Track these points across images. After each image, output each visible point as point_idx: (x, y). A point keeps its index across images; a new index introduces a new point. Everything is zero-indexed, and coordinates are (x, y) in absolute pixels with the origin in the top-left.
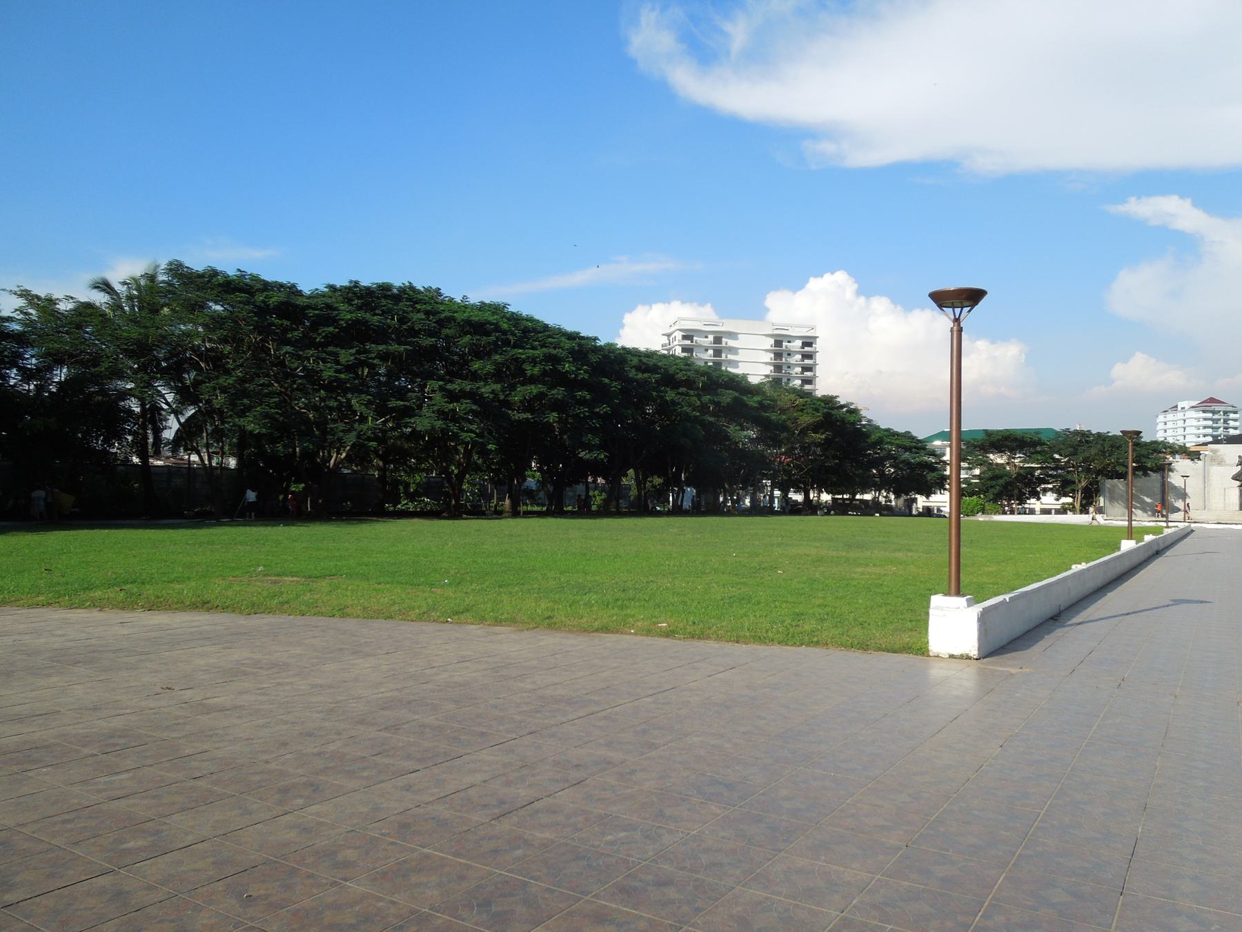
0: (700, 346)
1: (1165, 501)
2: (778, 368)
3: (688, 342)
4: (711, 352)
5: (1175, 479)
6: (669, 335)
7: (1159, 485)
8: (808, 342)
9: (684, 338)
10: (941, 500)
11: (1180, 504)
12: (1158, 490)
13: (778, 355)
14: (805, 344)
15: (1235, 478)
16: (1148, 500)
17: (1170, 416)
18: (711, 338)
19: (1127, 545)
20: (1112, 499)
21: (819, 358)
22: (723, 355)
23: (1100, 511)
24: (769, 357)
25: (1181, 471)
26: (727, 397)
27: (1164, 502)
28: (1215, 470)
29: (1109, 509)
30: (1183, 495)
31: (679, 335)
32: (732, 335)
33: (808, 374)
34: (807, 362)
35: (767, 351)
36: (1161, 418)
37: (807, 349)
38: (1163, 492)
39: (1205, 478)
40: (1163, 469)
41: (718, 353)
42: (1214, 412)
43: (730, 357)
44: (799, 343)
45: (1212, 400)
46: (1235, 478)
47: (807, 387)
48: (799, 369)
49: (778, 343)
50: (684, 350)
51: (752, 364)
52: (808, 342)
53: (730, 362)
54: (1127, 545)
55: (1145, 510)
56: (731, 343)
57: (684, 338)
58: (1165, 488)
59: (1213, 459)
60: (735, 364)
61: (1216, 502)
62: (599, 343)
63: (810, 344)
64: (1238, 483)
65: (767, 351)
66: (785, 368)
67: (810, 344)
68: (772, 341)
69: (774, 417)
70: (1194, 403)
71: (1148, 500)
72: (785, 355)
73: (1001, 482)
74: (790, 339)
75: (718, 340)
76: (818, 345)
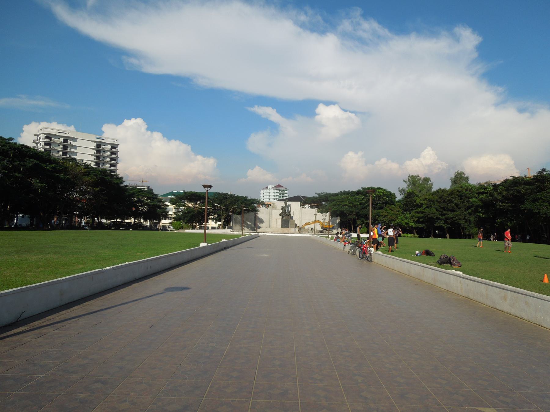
0: (55, 143)
1: (256, 224)
2: (98, 158)
3: (49, 140)
5: (260, 215)
6: (37, 136)
7: (253, 217)
8: (114, 147)
10: (165, 223)
11: (260, 225)
12: (253, 220)
13: (98, 151)
14: (112, 148)
15: (280, 215)
16: (249, 223)
17: (265, 191)
18: (62, 139)
19: (203, 244)
20: (236, 223)
21: (119, 155)
22: (69, 149)
23: (230, 228)
24: (93, 152)
25: (262, 212)
26: (30, 163)
27: (255, 224)
28: (274, 211)
29: (234, 227)
30: (262, 222)
31: (43, 136)
33: (114, 162)
34: (113, 156)
35: (92, 149)
36: (262, 192)
37: (113, 150)
38: (255, 220)
39: (270, 215)
40: (255, 211)
41: (65, 147)
42: (280, 190)
43: (72, 150)
44: (109, 147)
45: (279, 186)
46: (280, 215)
47: (112, 168)
48: (109, 159)
49: (99, 145)
50: (46, 144)
51: (85, 154)
52: (114, 147)
53: (72, 152)
54: (203, 244)
55: (248, 228)
56: (73, 143)
57: (46, 138)
59: (273, 207)
60: (75, 154)
61: (273, 224)
63: (115, 148)
64: (281, 217)
65: (92, 149)
66: (102, 158)
67: (115, 148)
68: (95, 144)
69: (62, 176)
70: (273, 186)
71: (249, 223)
73: (190, 214)
74: (105, 144)
75: (66, 141)
76: (119, 149)
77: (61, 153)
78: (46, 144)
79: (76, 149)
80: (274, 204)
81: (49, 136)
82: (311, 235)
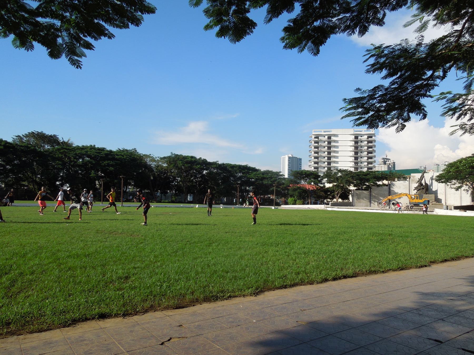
0: (321, 141)
2: (356, 148)
3: (317, 139)
4: (326, 143)
9: (315, 138)
13: (356, 142)
14: (368, 137)
18: (326, 137)
31: (313, 137)
32: (336, 135)
34: (370, 144)
35: (351, 141)
37: (369, 139)
41: (329, 143)
44: (366, 137)
49: (356, 137)
50: (315, 142)
57: (315, 138)
58: (390, 192)
59: (413, 181)
62: (74, 146)
63: (371, 137)
65: (351, 141)
68: (353, 137)
72: (359, 142)
74: (362, 136)
75: (329, 138)
77: (326, 148)
78: (315, 142)
79: (338, 143)
80: (414, 177)
81: (317, 137)
82: (392, 212)
